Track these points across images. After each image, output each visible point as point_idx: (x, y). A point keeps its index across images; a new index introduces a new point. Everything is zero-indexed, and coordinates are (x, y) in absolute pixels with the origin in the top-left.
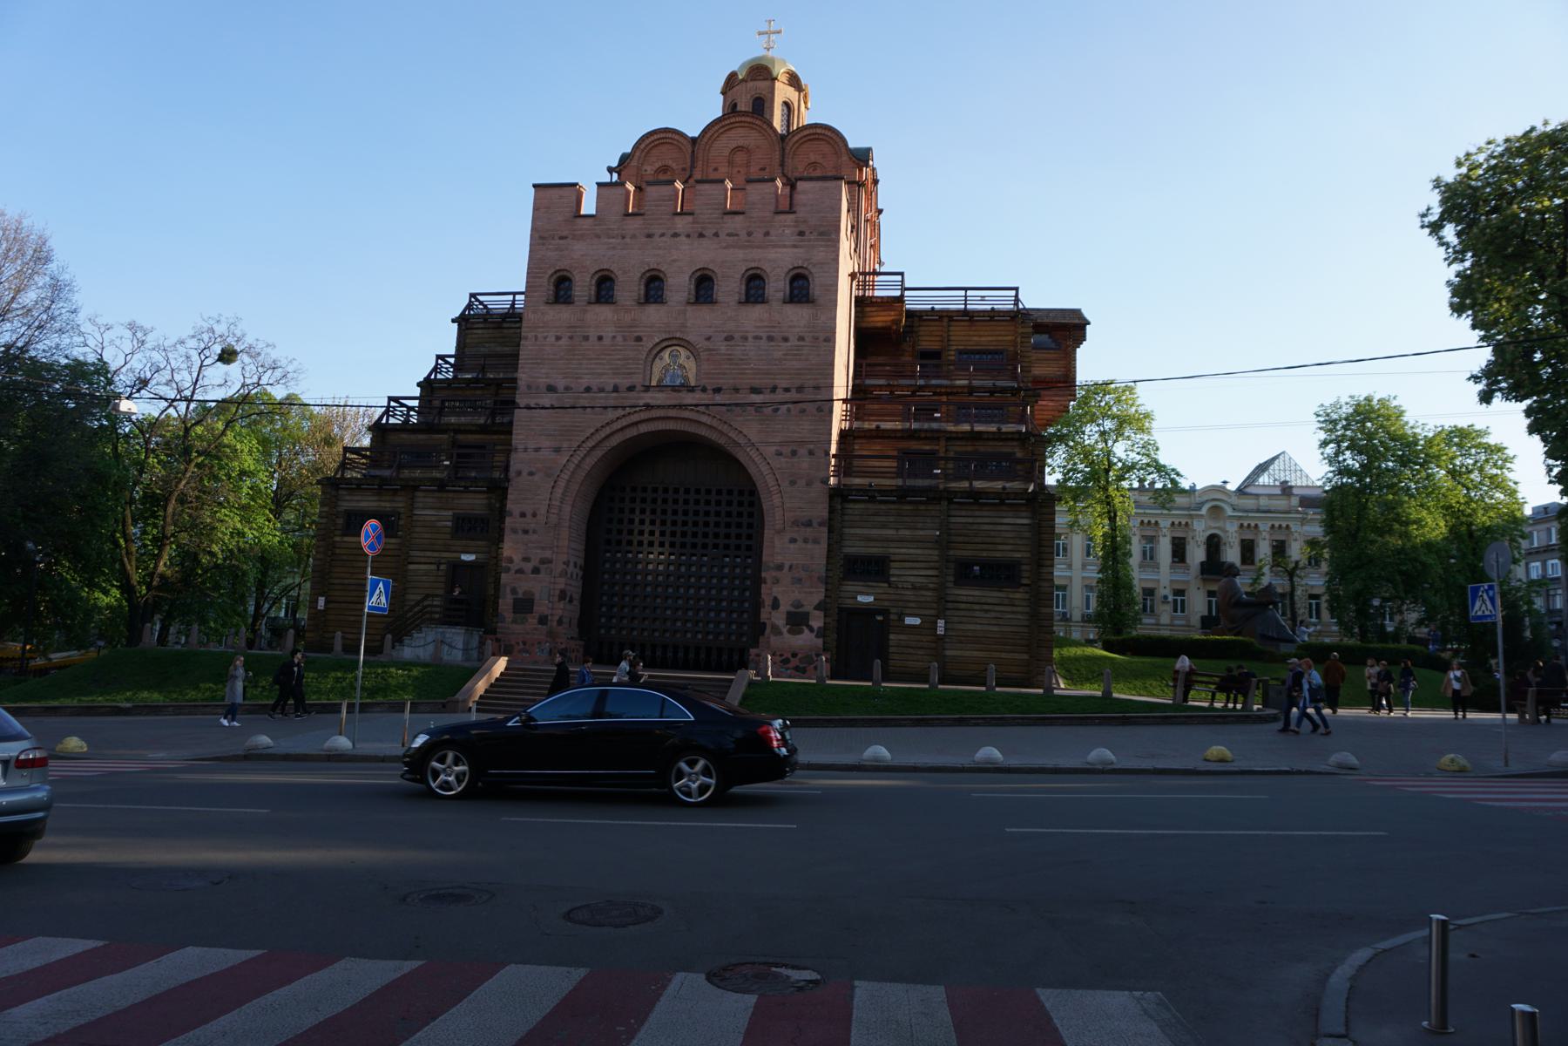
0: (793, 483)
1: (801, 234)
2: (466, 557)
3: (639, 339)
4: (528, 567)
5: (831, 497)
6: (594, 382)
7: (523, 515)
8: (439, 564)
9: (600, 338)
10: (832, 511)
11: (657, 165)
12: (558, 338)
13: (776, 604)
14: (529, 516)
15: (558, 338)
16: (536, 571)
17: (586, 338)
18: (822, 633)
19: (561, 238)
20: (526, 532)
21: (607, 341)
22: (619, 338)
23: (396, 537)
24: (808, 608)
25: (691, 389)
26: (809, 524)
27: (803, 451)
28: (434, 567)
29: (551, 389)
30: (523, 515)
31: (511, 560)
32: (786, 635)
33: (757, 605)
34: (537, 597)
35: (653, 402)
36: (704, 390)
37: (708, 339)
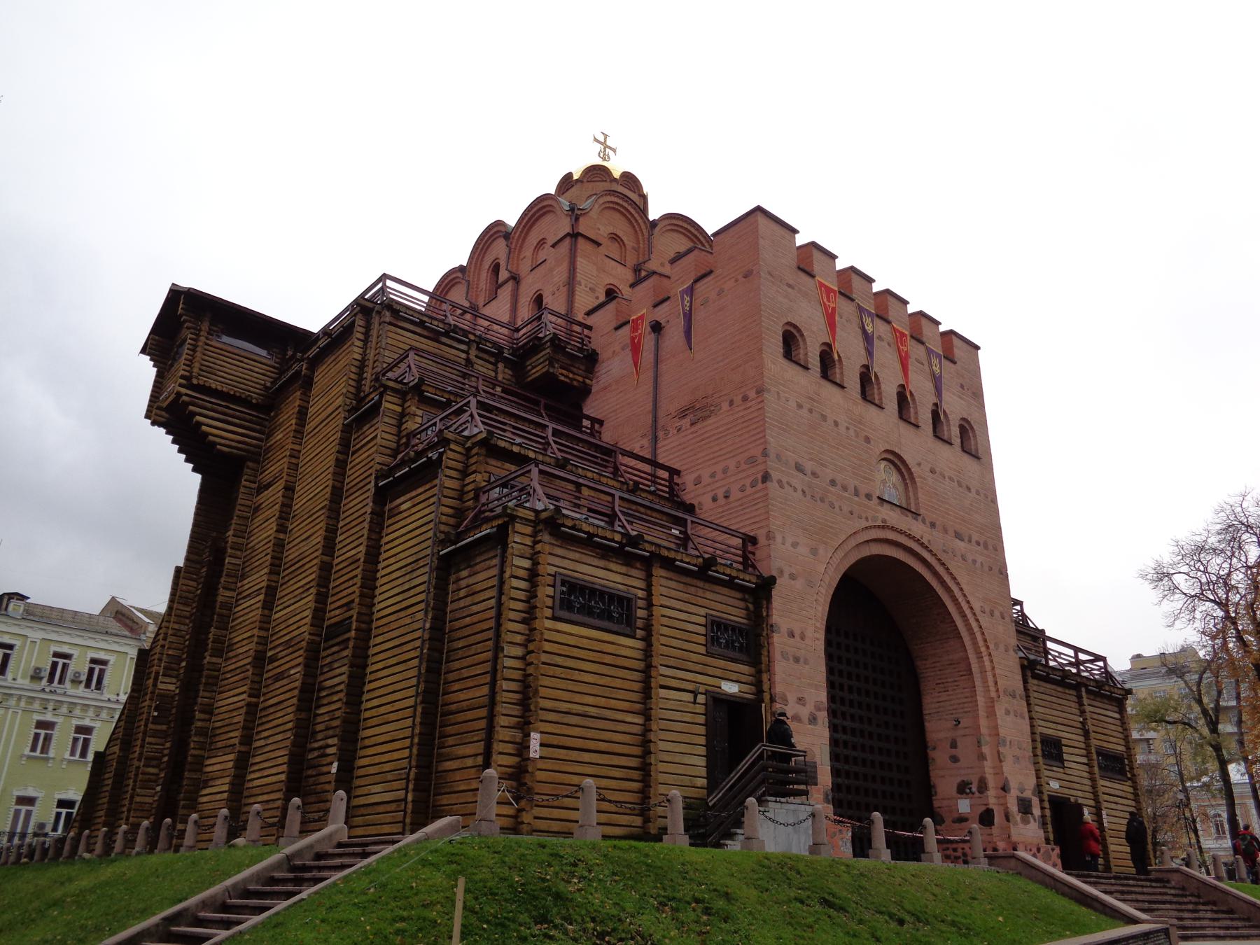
0: (996, 645)
1: (962, 386)
2: (730, 688)
3: (867, 440)
4: (804, 712)
5: (1023, 667)
6: (839, 478)
7: (792, 635)
8: (695, 693)
9: (836, 423)
10: (1025, 682)
11: (611, 230)
12: (800, 406)
13: (1005, 788)
14: (797, 638)
15: (800, 406)
16: (813, 720)
17: (824, 418)
18: (1044, 824)
19: (789, 285)
20: (797, 660)
21: (842, 429)
22: (852, 432)
23: (633, 637)
24: (1028, 794)
25: (916, 515)
26: (1014, 697)
27: (997, 613)
28: (689, 697)
29: (799, 468)
30: (792, 635)
31: (785, 701)
32: (1021, 826)
33: (927, 789)
34: (819, 763)
35: (891, 522)
36: (924, 521)
37: (919, 464)
